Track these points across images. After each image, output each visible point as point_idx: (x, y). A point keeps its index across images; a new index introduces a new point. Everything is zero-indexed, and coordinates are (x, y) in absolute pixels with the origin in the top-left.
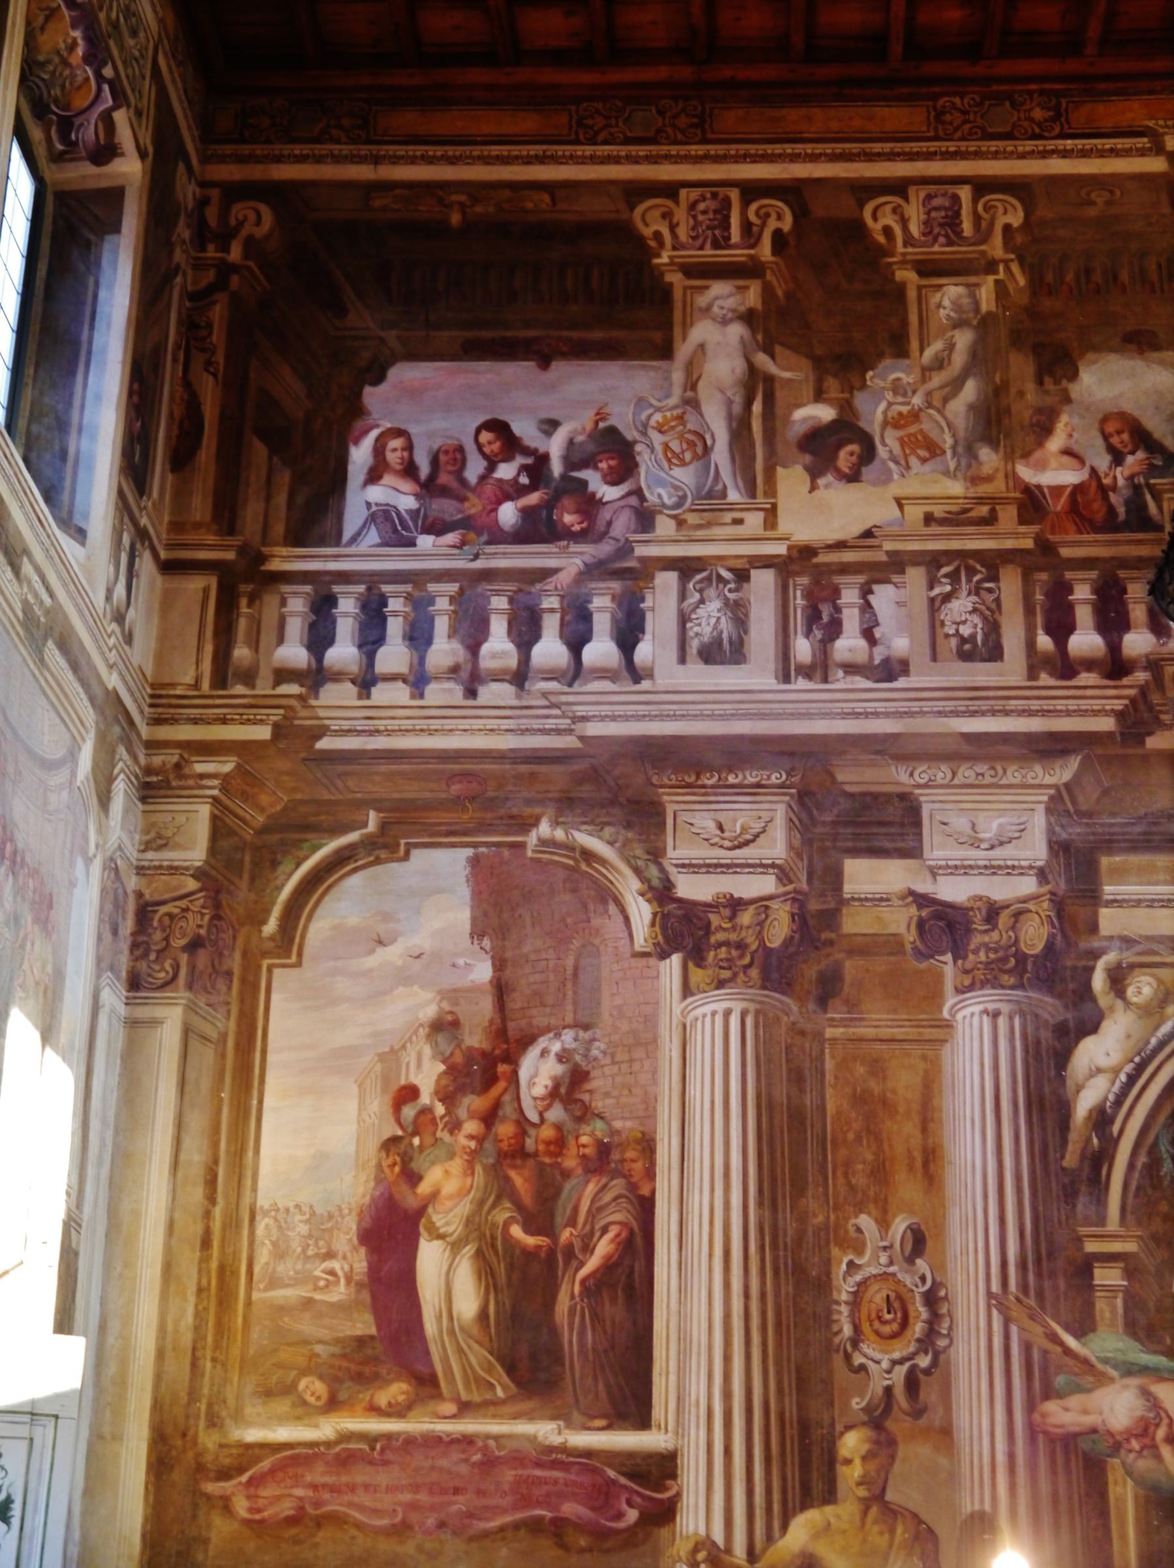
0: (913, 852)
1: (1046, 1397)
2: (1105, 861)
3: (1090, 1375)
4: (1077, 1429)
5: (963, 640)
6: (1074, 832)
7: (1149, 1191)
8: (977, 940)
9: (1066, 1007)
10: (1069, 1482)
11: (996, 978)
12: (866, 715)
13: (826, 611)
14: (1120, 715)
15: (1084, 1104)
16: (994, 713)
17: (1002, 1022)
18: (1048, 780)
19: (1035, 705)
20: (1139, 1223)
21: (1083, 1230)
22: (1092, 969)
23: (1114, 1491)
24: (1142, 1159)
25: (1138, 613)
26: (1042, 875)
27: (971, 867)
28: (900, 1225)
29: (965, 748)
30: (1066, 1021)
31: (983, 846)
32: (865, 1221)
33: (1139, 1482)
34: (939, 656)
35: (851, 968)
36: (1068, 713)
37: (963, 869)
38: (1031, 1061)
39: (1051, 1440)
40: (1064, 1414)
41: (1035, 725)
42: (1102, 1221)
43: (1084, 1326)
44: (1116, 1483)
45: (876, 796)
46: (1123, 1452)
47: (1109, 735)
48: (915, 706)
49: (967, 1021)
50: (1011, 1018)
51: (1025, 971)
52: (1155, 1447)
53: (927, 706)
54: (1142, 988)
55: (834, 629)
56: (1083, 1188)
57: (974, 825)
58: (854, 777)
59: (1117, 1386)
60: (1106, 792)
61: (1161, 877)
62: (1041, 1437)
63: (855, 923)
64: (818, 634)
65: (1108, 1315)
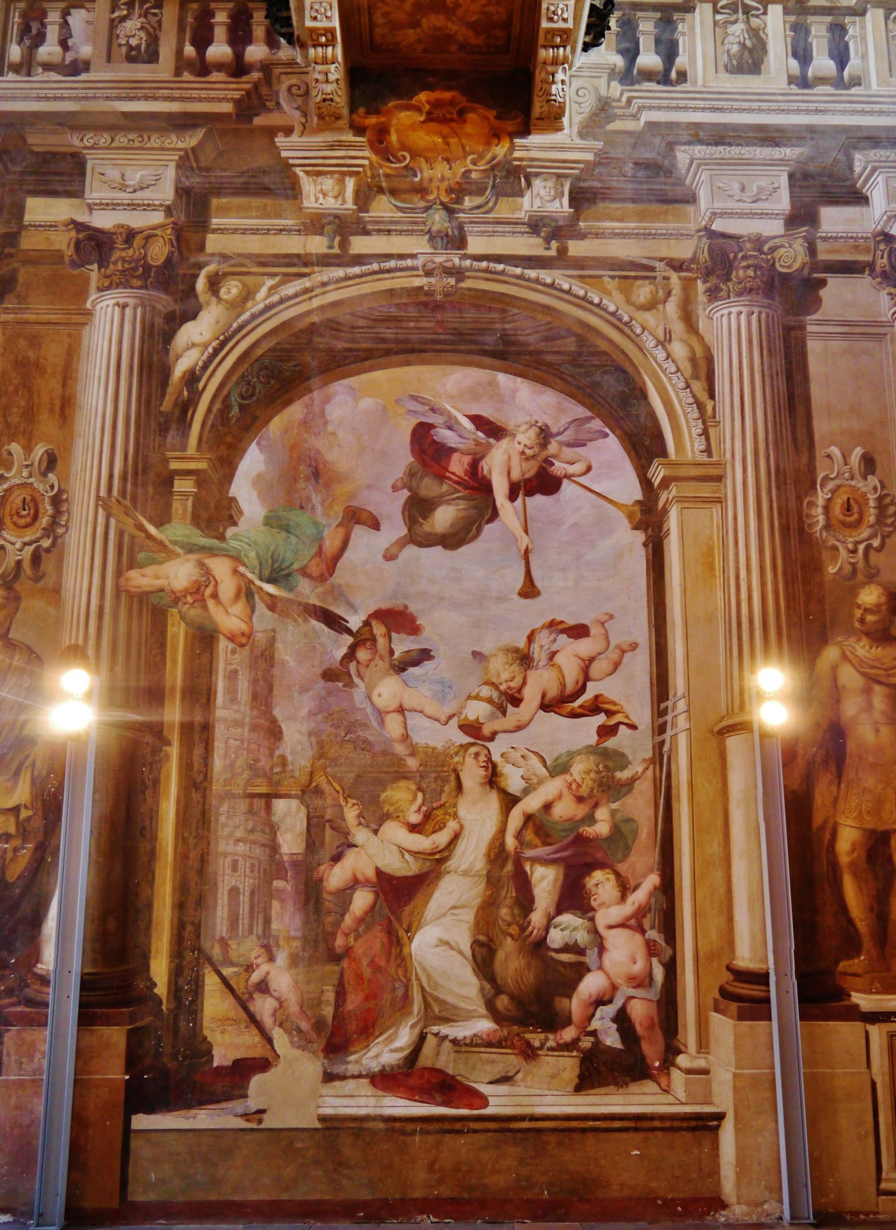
0: (77, 193)
1: (131, 567)
2: (215, 202)
4: (149, 589)
5: (131, 48)
6: (194, 181)
7: (220, 428)
8: (116, 255)
9: (176, 301)
10: (140, 626)
11: (127, 281)
12: (55, 99)
13: (35, 27)
14: (238, 102)
15: (180, 369)
16: (146, 98)
17: (128, 311)
18: (180, 145)
19: (177, 94)
20: (210, 449)
21: (169, 454)
22: (196, 276)
23: (171, 630)
24: (218, 406)
25: (259, 31)
26: (169, 211)
27: (118, 204)
28: (39, 450)
29: (123, 122)
30: (174, 311)
31: (129, 190)
32: (15, 448)
33: (190, 624)
34: (112, 59)
35: (23, 274)
36: (200, 100)
38: (146, 337)
39: (131, 596)
40: (140, 580)
41: (175, 107)
42: (184, 448)
43: (161, 521)
44: (173, 625)
45: (54, 155)
46: (180, 604)
47: (228, 115)
48: (91, 93)
50: (135, 309)
51: (149, 277)
52: (203, 600)
53: (99, 93)
54: (231, 289)
55: (40, 39)
56: (174, 426)
57: (123, 175)
58: (38, 141)
59: (181, 560)
60: (220, 154)
61: (254, 213)
62: (123, 594)
63: (29, 242)
64: (27, 42)
65: (180, 512)
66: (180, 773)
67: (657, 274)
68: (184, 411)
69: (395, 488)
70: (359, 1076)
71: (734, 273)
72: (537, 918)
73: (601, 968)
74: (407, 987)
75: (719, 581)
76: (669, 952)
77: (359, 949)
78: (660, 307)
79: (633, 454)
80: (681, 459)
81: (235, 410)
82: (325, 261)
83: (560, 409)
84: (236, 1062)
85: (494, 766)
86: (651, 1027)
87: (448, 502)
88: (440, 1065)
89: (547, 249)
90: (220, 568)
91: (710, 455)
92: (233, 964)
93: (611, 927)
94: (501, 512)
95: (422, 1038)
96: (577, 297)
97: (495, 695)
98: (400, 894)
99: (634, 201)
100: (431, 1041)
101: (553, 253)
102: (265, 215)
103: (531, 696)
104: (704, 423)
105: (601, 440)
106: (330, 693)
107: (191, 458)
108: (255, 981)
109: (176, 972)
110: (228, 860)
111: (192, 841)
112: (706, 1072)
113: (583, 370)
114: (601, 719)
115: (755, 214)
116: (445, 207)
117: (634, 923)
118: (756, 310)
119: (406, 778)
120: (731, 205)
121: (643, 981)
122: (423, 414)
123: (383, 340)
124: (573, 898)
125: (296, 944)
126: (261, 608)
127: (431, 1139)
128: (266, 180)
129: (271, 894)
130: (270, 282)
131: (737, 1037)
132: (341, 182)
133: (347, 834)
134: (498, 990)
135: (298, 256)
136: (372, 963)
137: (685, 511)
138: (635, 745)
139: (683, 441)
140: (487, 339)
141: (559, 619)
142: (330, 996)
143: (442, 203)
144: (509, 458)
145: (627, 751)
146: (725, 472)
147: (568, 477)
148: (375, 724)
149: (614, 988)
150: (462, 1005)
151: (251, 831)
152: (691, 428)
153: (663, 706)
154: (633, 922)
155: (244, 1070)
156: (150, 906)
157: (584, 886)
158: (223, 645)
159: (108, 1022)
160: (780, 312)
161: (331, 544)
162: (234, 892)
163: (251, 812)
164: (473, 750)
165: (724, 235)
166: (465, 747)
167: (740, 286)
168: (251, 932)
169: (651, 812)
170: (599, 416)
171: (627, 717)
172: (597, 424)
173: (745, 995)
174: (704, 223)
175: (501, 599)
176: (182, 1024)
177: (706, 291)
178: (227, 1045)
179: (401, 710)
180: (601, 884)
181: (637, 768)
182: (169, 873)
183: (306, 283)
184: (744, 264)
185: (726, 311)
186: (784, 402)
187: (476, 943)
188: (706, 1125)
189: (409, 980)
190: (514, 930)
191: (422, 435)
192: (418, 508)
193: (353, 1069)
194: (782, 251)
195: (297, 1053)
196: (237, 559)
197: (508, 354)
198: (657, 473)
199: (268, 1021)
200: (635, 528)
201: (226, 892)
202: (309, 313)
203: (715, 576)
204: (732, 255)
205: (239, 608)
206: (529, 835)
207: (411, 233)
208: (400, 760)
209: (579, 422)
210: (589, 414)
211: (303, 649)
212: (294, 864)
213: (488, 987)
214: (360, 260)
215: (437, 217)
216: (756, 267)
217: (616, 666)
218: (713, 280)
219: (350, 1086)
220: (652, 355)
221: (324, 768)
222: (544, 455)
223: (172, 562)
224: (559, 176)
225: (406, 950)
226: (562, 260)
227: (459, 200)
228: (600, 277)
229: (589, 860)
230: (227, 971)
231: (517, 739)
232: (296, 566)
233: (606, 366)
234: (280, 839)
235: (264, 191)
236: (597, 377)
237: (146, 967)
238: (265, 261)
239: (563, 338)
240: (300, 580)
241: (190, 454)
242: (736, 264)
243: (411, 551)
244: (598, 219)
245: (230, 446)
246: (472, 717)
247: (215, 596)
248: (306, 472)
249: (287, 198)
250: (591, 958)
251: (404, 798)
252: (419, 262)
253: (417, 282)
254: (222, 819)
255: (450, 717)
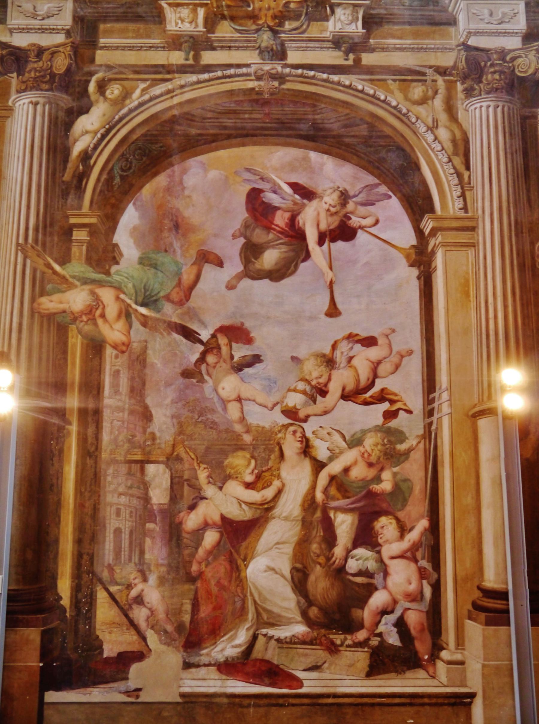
1: (42, 295)
2: (102, 26)
3: (65, 285)
4: (55, 311)
6: (87, 11)
7: (106, 192)
8: (30, 66)
9: (74, 100)
10: (49, 337)
11: (38, 85)
15: (77, 149)
17: (39, 107)
20: (99, 209)
21: (69, 212)
22: (88, 82)
23: (71, 341)
24: (104, 176)
26: (68, 33)
27: (31, 29)
30: (73, 107)
31: (39, 18)
37: (27, 30)
38: (52, 127)
39: (42, 316)
40: (49, 304)
42: (80, 208)
43: (64, 261)
44: (73, 337)
46: (78, 322)
49: (21, 107)
50: (44, 106)
51: (54, 82)
52: (94, 319)
54: (114, 91)
56: (72, 192)
57: (35, 7)
59: (78, 290)
61: (130, 34)
62: (36, 315)
65: (78, 254)
66: (78, 445)
67: (427, 78)
68: (80, 180)
69: (234, 237)
70: (209, 665)
71: (484, 77)
72: (339, 551)
73: (385, 587)
74: (244, 601)
75: (473, 304)
76: (435, 576)
77: (209, 573)
78: (430, 102)
79: (410, 211)
80: (445, 215)
81: (117, 180)
82: (183, 69)
83: (356, 178)
84: (120, 654)
85: (307, 440)
86: (422, 630)
87: (273, 247)
88: (268, 656)
89: (346, 60)
90: (107, 295)
91: (466, 211)
92: (117, 584)
93: (393, 558)
94: (312, 254)
95: (255, 637)
96: (368, 95)
97: (308, 388)
98: (238, 533)
99: (410, 24)
100: (261, 640)
101: (350, 62)
102: (138, 36)
103: (335, 389)
104: (462, 188)
105: (386, 201)
106: (187, 387)
107: (85, 215)
108: (134, 596)
109: (76, 589)
110: (114, 508)
111: (87, 494)
112: (462, 663)
113: (372, 149)
114: (386, 406)
115: (500, 33)
116: (271, 29)
117: (409, 555)
118: (501, 104)
119: (243, 449)
120: (482, 26)
121: (416, 597)
122: (255, 182)
123: (225, 128)
124: (365, 536)
125: (163, 569)
126: (136, 325)
127: (262, 710)
128: (140, 10)
129: (145, 533)
130: (142, 86)
131: (485, 638)
132: (195, 11)
133: (200, 489)
134: (310, 603)
135: (163, 66)
136: (218, 584)
137: (448, 253)
138: (410, 425)
139: (446, 201)
140: (302, 126)
141: (355, 332)
142: (188, 607)
143: (269, 26)
144: (318, 214)
145: (405, 430)
146: (478, 224)
147: (361, 228)
148: (220, 409)
149: (395, 602)
150: (284, 614)
151: (131, 487)
152: (453, 192)
153: (431, 396)
154: (409, 554)
155: (126, 659)
156: (57, 541)
157: (373, 528)
158: (109, 352)
159: (28, 625)
160: (518, 105)
161: (187, 277)
162: (118, 532)
163: (130, 473)
164: (292, 428)
165: (477, 49)
166: (286, 427)
167: (489, 87)
168: (130, 560)
169: (422, 474)
170: (385, 183)
171: (405, 404)
172: (383, 189)
173: (491, 607)
174: (462, 40)
175: (312, 318)
176: (81, 626)
177: (464, 91)
178: (113, 641)
179: (239, 399)
180: (386, 527)
181: (411, 442)
182: (71, 517)
183: (169, 86)
184: (492, 70)
185: (478, 105)
186: (521, 172)
187: (294, 569)
188: (462, 702)
189: (245, 596)
190: (322, 560)
191: (254, 197)
192: (251, 251)
193: (205, 660)
194: (520, 60)
195: (164, 648)
196: (119, 289)
197: (318, 138)
198: (428, 225)
199: (143, 625)
200: (411, 265)
201: (112, 531)
202: (171, 108)
203: (470, 301)
204: (483, 64)
205: (121, 325)
206: (333, 491)
207: (246, 48)
208: (238, 436)
209: (370, 187)
210: (377, 181)
211: (166, 355)
212: (161, 511)
213: (303, 601)
214: (208, 68)
215: (265, 37)
216: (501, 72)
217: (397, 367)
218: (469, 83)
219: (203, 671)
220: (423, 138)
221: (183, 442)
222: (343, 212)
223: (71, 292)
224: (355, 6)
225: (243, 574)
226: (357, 68)
227: (281, 24)
228: (385, 80)
229: (377, 509)
230: (113, 589)
231: (324, 420)
232: (162, 294)
233: (389, 146)
234: (151, 493)
235: (138, 18)
236: (383, 154)
237: (54, 586)
238: (139, 70)
239: (358, 125)
240: (165, 304)
241: (84, 212)
242: (486, 70)
243: (246, 283)
244: (384, 38)
245: (113, 206)
246: (291, 404)
247: (103, 316)
248: (169, 225)
249: (155, 23)
250: (378, 580)
251: (242, 464)
252: (252, 70)
253: (251, 85)
254: (109, 479)
255: (275, 405)
